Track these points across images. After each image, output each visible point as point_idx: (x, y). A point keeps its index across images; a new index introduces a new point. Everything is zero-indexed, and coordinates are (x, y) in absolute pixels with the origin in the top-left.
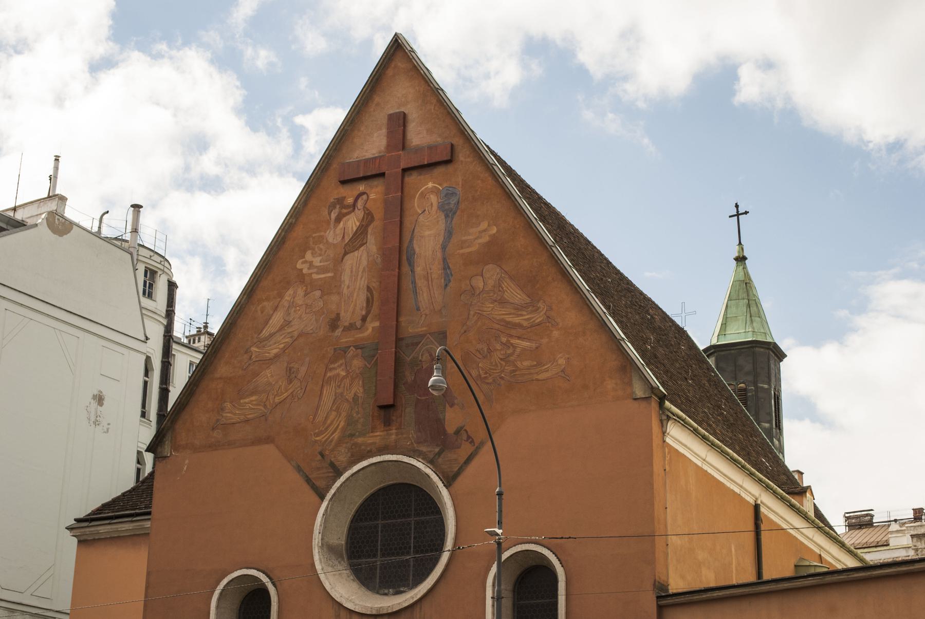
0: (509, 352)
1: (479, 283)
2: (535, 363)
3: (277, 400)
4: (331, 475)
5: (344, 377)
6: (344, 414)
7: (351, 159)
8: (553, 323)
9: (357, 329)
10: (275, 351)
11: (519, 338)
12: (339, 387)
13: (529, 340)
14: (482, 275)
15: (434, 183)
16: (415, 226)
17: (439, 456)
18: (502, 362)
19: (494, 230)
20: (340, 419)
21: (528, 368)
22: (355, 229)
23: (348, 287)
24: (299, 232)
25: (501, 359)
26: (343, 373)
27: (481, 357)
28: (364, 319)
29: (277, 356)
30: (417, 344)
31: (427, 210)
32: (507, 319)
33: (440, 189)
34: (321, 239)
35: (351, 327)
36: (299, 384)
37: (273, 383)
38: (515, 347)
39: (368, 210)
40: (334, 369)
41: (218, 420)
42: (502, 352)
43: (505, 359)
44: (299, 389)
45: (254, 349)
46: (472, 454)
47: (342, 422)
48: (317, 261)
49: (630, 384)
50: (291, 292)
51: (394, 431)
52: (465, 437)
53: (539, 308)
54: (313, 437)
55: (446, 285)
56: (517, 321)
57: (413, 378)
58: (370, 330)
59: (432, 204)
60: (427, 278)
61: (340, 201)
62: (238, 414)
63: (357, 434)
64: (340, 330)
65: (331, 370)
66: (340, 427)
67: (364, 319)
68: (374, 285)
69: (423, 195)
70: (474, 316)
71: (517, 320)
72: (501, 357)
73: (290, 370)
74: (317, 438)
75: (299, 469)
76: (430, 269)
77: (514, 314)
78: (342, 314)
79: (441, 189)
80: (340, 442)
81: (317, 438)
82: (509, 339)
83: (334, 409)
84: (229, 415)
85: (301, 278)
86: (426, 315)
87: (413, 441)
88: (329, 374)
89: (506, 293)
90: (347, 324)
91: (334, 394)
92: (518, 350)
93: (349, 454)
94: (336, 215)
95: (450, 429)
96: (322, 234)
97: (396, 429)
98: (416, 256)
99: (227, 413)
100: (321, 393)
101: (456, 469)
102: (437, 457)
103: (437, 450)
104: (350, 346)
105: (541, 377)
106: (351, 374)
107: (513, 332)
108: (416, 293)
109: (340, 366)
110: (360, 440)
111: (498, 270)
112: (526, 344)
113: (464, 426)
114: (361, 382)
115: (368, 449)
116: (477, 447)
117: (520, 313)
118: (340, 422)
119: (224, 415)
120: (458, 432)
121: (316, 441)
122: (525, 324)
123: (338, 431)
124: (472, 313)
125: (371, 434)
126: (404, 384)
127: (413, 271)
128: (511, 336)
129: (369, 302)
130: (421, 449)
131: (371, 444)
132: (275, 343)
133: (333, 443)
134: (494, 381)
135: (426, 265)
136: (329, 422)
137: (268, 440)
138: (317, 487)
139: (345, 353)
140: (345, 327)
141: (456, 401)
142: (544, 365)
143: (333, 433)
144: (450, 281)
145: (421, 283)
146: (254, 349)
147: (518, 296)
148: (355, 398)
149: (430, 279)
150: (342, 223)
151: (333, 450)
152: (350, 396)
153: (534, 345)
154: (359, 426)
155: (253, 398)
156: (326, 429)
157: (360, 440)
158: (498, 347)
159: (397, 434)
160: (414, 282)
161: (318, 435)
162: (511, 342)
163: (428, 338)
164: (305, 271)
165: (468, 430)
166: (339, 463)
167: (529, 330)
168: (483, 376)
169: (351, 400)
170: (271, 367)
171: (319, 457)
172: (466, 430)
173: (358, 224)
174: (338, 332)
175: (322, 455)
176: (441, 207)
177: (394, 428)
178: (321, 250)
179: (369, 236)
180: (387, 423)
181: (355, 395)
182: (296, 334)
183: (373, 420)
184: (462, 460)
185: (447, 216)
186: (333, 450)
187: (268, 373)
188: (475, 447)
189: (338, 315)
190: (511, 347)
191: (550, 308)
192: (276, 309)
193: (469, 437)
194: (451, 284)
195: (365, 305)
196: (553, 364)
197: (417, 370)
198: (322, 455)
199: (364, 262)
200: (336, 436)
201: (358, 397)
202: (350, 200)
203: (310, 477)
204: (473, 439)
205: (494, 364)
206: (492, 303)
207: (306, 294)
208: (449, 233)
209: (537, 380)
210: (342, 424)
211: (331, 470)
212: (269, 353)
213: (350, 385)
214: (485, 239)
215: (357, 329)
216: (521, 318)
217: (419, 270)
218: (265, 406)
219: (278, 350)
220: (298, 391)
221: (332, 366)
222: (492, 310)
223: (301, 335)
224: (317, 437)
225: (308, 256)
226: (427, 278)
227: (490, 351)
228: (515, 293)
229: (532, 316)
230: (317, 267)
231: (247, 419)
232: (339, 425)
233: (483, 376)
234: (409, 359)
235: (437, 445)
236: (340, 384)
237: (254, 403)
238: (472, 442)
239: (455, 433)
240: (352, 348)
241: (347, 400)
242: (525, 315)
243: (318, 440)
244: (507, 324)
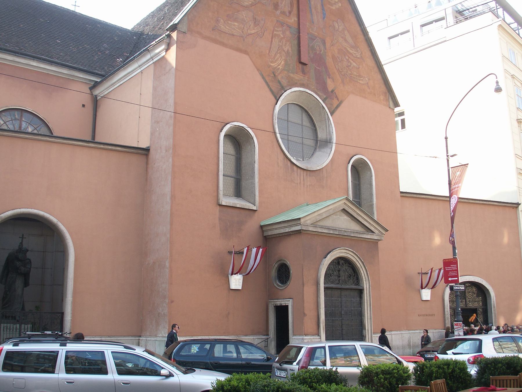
0: (349, 64)
4: (279, 87)
6: (283, 58)
9: (287, 16)
10: (246, 3)
11: (352, 60)
12: (280, 41)
17: (326, 100)
18: (347, 68)
21: (356, 76)
25: (346, 66)
27: (339, 61)
28: (290, 13)
30: (315, 39)
32: (348, 49)
35: (283, 13)
36: (260, 29)
38: (351, 64)
44: (260, 32)
46: (338, 105)
47: (282, 62)
55: (324, 18)
56: (351, 52)
62: (227, 28)
66: (282, 64)
71: (351, 51)
74: (271, 64)
75: (263, 78)
77: (350, 48)
78: (280, 4)
81: (271, 64)
84: (222, 26)
87: (315, 87)
92: (352, 66)
93: (287, 81)
95: (330, 90)
97: (308, 78)
99: (221, 24)
100: (272, 41)
103: (325, 97)
105: (361, 82)
106: (286, 38)
110: (292, 75)
112: (354, 64)
113: (334, 90)
114: (290, 45)
115: (296, 82)
116: (340, 103)
117: (352, 49)
119: (219, 25)
120: (332, 91)
121: (271, 66)
122: (354, 55)
123: (281, 65)
125: (297, 75)
130: (318, 93)
134: (344, 74)
137: (246, 52)
138: (273, 91)
141: (330, 76)
142: (361, 78)
143: (279, 65)
151: (279, 74)
152: (286, 49)
155: (236, 24)
157: (292, 75)
158: (345, 60)
160: (310, 8)
161: (272, 62)
163: (318, 39)
165: (336, 92)
167: (355, 58)
170: (245, 11)
172: (335, 92)
174: (278, 12)
175: (273, 73)
177: (306, 76)
180: (304, 72)
183: (297, 68)
184: (335, 106)
186: (279, 74)
187: (244, 14)
188: (339, 102)
189: (277, 3)
191: (362, 53)
193: (336, 97)
194: (326, 18)
196: (364, 78)
197: (315, 53)
198: (273, 73)
200: (280, 67)
203: (269, 84)
204: (338, 98)
206: (342, 38)
209: (359, 83)
210: (283, 63)
211: (279, 85)
212: (243, 3)
213: (285, 44)
214: (337, 7)
216: (353, 51)
218: (243, 32)
219: (248, 4)
220: (260, 33)
222: (342, 41)
224: (271, 63)
229: (356, 53)
231: (232, 34)
233: (340, 70)
235: (325, 95)
236: (281, 41)
237: (237, 27)
238: (338, 99)
241: (284, 51)
242: (353, 51)
243: (272, 66)
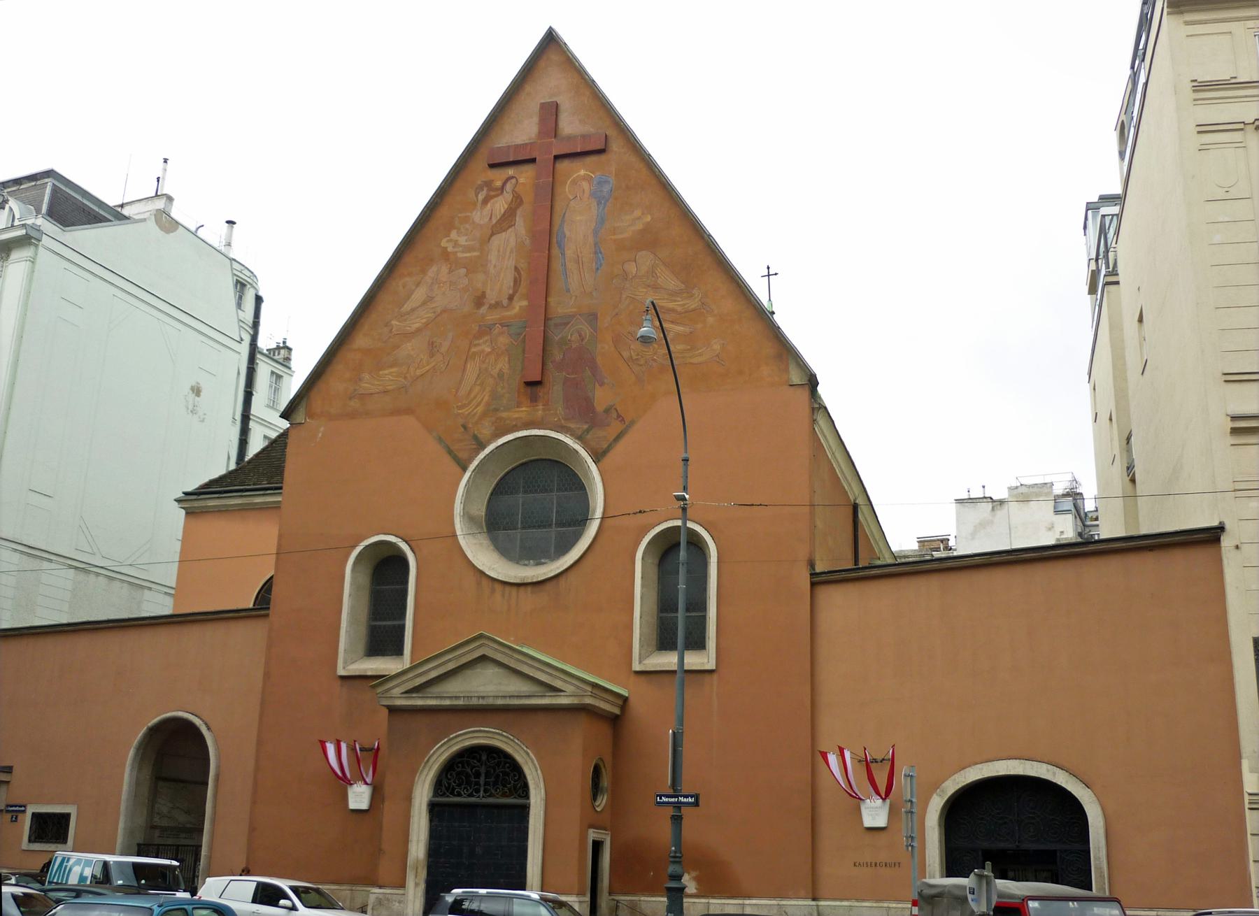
2: (689, 347)
3: (419, 372)
5: (489, 354)
6: (488, 389)
7: (499, 144)
8: (708, 309)
9: (503, 307)
10: (417, 325)
12: (484, 362)
14: (635, 262)
19: (649, 218)
20: (485, 393)
22: (503, 211)
23: (495, 266)
24: (444, 212)
28: (511, 298)
29: (419, 330)
30: (568, 323)
34: (466, 220)
35: (497, 305)
37: (415, 356)
39: (516, 193)
40: (479, 345)
41: (355, 390)
45: (394, 322)
48: (462, 240)
49: (787, 370)
50: (434, 268)
51: (541, 407)
52: (614, 415)
53: (694, 294)
57: (561, 357)
58: (517, 308)
59: (584, 190)
61: (488, 184)
64: (488, 306)
65: (475, 345)
67: (511, 298)
68: (522, 266)
69: (574, 182)
73: (433, 343)
74: (460, 411)
78: (488, 292)
81: (460, 411)
83: (478, 383)
85: (446, 255)
86: (576, 297)
88: (473, 350)
90: (493, 302)
93: (493, 428)
94: (483, 197)
95: (600, 407)
96: (468, 214)
100: (464, 370)
101: (606, 446)
102: (586, 433)
103: (586, 427)
105: (695, 360)
110: (505, 415)
117: (673, 298)
118: (485, 395)
120: (607, 411)
121: (459, 414)
122: (679, 309)
124: (624, 296)
126: (551, 362)
127: (563, 254)
129: (517, 282)
131: (517, 419)
132: (417, 318)
134: (646, 362)
137: (408, 411)
140: (490, 305)
141: (606, 381)
144: (601, 265)
145: (571, 266)
146: (394, 322)
148: (501, 375)
150: (489, 205)
153: (687, 330)
156: (469, 403)
159: (544, 410)
164: (450, 249)
165: (618, 409)
168: (635, 357)
169: (496, 376)
171: (462, 429)
173: (506, 206)
174: (483, 310)
175: (465, 427)
177: (541, 404)
178: (467, 229)
179: (517, 219)
180: (534, 399)
182: (439, 310)
188: (625, 426)
192: (418, 285)
193: (619, 416)
195: (512, 284)
198: (465, 427)
199: (512, 243)
202: (499, 184)
203: (451, 448)
204: (623, 418)
207: (450, 271)
210: (486, 398)
214: (639, 226)
215: (503, 307)
217: (569, 253)
218: (405, 378)
221: (477, 342)
223: (444, 311)
225: (454, 234)
226: (578, 261)
230: (461, 246)
232: (482, 399)
233: (635, 357)
235: (586, 422)
237: (394, 374)
238: (623, 420)
239: (604, 412)
240: (498, 325)
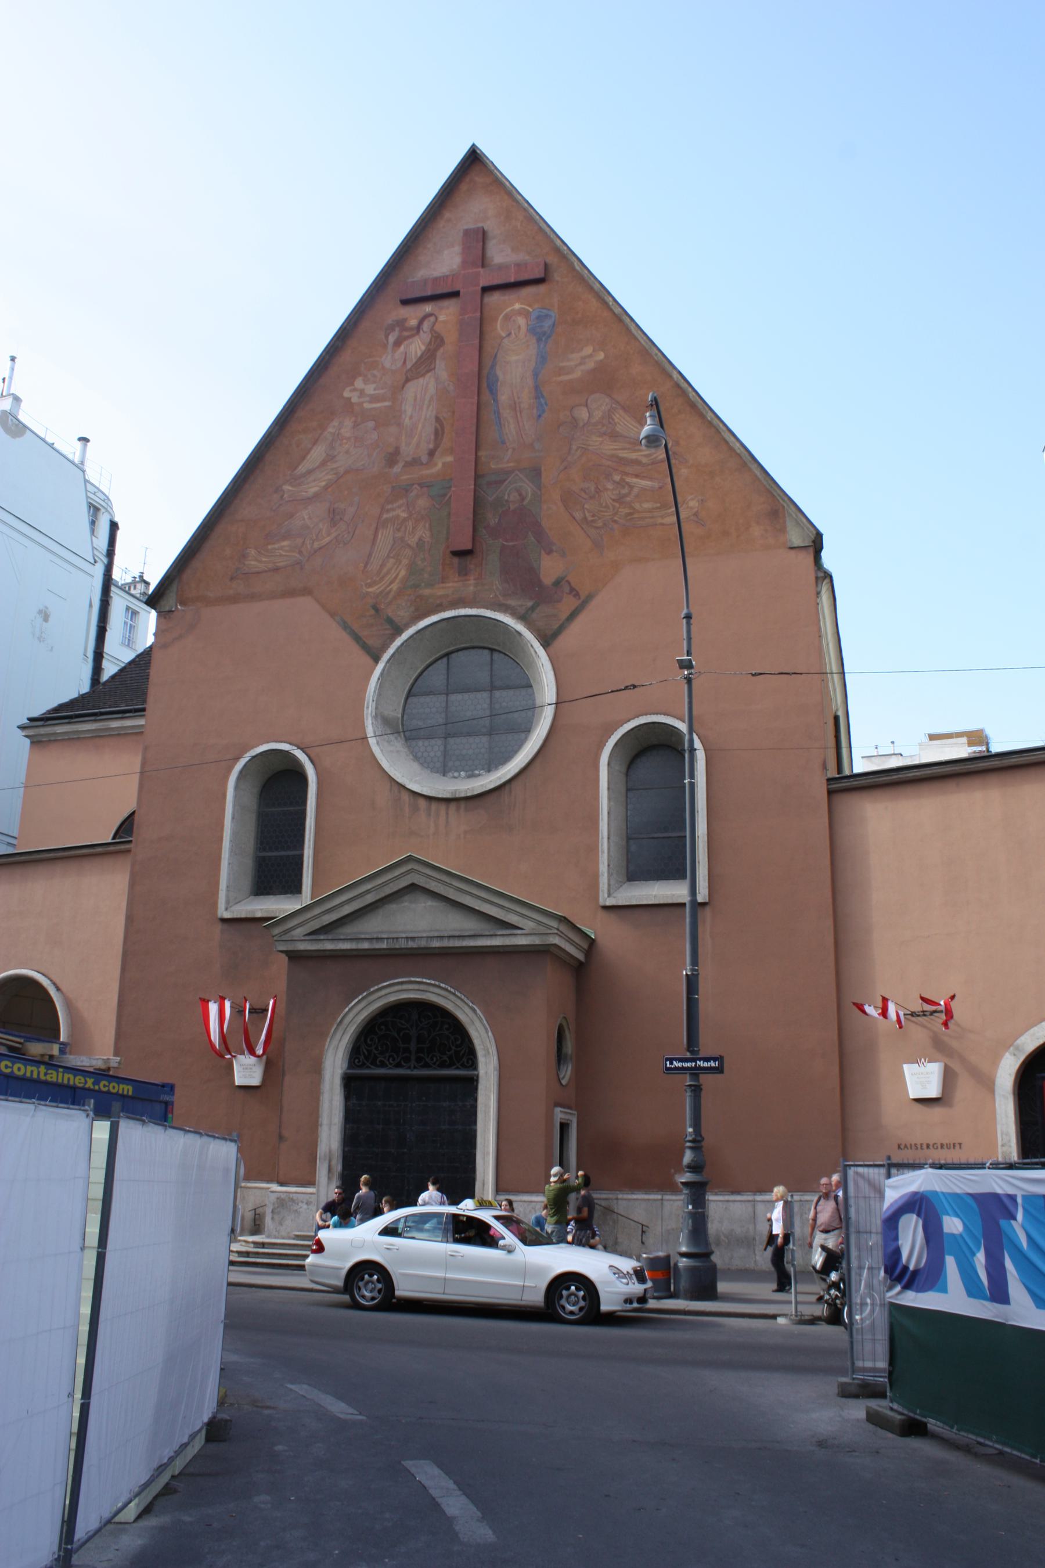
0: (625, 491)
1: (583, 414)
4: (387, 632)
5: (405, 520)
6: (405, 562)
9: (422, 464)
11: (637, 476)
13: (651, 479)
14: (587, 405)
15: (522, 304)
16: (498, 351)
19: (601, 356)
20: (400, 567)
21: (650, 511)
26: (404, 515)
28: (431, 454)
31: (513, 332)
32: (620, 455)
33: (528, 311)
38: (631, 487)
40: (393, 510)
42: (614, 492)
43: (620, 500)
54: (364, 588)
55: (540, 416)
56: (634, 457)
57: (497, 520)
58: (440, 465)
59: (519, 327)
60: (514, 407)
63: (423, 584)
64: (401, 465)
65: (388, 511)
66: (400, 576)
67: (431, 454)
69: (508, 318)
70: (576, 450)
72: (613, 497)
74: (370, 590)
75: (345, 626)
76: (519, 398)
77: (629, 449)
79: (531, 310)
80: (400, 593)
81: (370, 590)
82: (624, 477)
86: (514, 449)
88: (385, 516)
89: (618, 425)
90: (409, 459)
91: (392, 538)
92: (636, 490)
93: (412, 609)
98: (499, 383)
104: (413, 485)
107: (629, 469)
108: (500, 424)
109: (399, 507)
110: (427, 592)
111: (607, 400)
117: (637, 448)
118: (400, 571)
121: (368, 593)
122: (644, 460)
123: (397, 581)
124: (574, 447)
125: (444, 585)
127: (496, 400)
128: (627, 474)
133: (391, 596)
134: (605, 524)
135: (513, 394)
136: (385, 570)
139: (407, 491)
140: (406, 462)
143: (391, 583)
144: (544, 411)
145: (506, 413)
147: (635, 429)
149: (518, 409)
152: (413, 541)
154: (426, 576)
156: (382, 578)
158: (610, 486)
160: (498, 413)
161: (370, 585)
162: (627, 480)
163: (517, 475)
166: (399, 618)
167: (650, 467)
168: (590, 519)
171: (372, 612)
174: (397, 469)
176: (532, 331)
181: (420, 539)
185: (539, 340)
190: (627, 487)
195: (433, 437)
201: (424, 542)
205: (604, 505)
208: (542, 359)
210: (403, 573)
211: (388, 627)
214: (590, 365)
217: (504, 398)
221: (390, 506)
222: (601, 444)
224: (368, 588)
227: (598, 491)
228: (630, 426)
232: (398, 574)
233: (590, 519)
234: (490, 499)
236: (401, 527)
240: (414, 486)
243: (371, 592)
244: (622, 461)
